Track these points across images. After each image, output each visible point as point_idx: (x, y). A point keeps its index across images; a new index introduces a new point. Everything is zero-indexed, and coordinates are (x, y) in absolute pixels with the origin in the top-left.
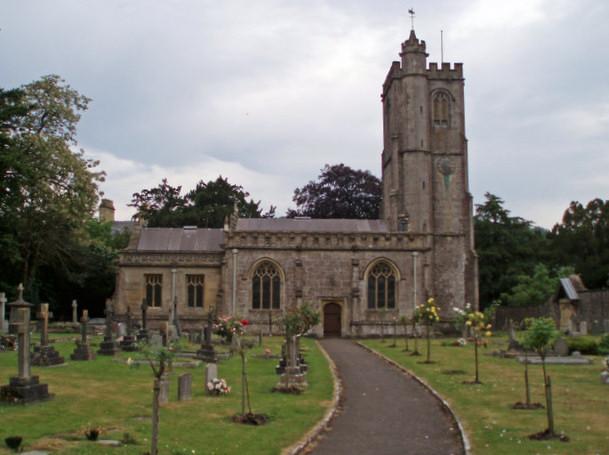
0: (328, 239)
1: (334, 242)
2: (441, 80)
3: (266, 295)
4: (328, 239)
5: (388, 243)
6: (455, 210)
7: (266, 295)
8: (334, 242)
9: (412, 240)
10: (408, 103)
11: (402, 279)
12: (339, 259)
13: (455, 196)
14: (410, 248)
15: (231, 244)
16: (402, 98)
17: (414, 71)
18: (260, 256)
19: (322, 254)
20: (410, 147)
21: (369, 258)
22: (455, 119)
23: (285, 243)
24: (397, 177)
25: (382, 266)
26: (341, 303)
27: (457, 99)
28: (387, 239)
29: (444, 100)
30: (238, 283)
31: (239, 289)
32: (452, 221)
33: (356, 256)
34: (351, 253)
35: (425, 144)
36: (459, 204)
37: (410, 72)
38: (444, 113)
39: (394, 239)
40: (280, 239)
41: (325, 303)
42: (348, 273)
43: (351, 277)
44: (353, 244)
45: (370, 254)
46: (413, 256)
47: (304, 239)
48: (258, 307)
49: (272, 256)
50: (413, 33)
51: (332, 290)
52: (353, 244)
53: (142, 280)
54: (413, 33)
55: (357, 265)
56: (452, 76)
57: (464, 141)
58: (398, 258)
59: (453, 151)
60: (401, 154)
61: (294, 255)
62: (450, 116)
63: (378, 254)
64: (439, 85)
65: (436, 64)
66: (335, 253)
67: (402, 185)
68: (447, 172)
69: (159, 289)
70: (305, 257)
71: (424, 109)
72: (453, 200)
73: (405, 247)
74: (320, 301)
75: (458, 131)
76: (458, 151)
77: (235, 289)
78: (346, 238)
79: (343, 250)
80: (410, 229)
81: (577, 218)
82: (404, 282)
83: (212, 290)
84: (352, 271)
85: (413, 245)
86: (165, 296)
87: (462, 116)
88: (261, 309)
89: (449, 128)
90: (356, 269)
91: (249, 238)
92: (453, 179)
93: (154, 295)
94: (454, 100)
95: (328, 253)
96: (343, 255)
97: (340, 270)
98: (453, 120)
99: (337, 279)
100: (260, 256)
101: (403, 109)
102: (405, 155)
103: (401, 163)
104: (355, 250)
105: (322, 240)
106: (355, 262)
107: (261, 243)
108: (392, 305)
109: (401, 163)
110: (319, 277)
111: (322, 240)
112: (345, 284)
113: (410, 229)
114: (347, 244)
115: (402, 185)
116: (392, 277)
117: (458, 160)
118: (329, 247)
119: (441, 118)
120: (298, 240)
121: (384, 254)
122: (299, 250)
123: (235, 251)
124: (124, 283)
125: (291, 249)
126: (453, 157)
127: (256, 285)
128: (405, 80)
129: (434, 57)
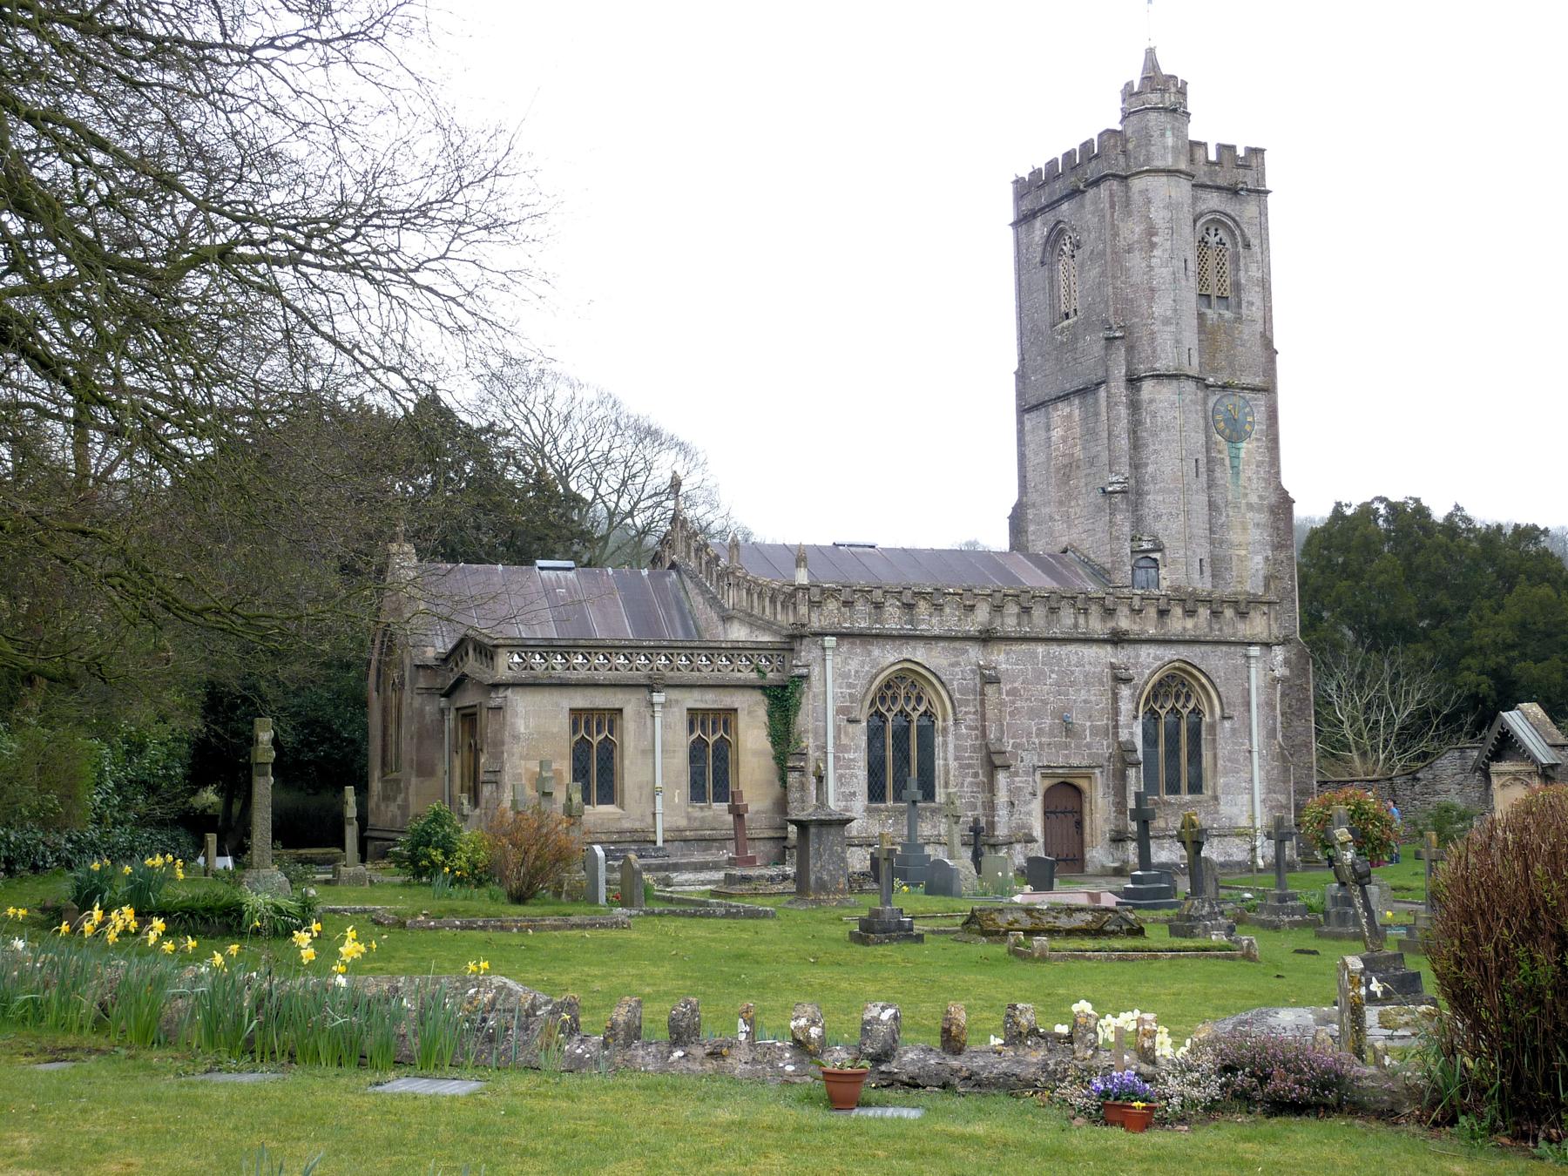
0: (1053, 610)
1: (1067, 618)
2: (1218, 188)
3: (1173, 752)
4: (1053, 610)
5: (1189, 623)
6: (1255, 535)
7: (1173, 752)
8: (1067, 618)
9: (1243, 615)
10: (1153, 246)
11: (1224, 718)
12: (1080, 664)
13: (1254, 499)
14: (1239, 637)
15: (816, 622)
16: (1132, 230)
17: (1169, 162)
18: (888, 657)
19: (1040, 649)
20: (1161, 366)
21: (1149, 662)
22: (1252, 295)
23: (951, 620)
24: (1124, 443)
25: (1174, 684)
26: (1083, 783)
27: (1254, 242)
28: (1190, 613)
29: (1220, 242)
30: (838, 729)
31: (839, 747)
32: (1252, 563)
33: (1120, 656)
34: (1109, 648)
35: (1195, 361)
36: (1263, 517)
37: (1159, 164)
38: (1220, 273)
39: (1204, 612)
40: (939, 608)
41: (1048, 783)
42: (1105, 702)
43: (1116, 712)
44: (1111, 624)
45: (1153, 650)
46: (1248, 657)
47: (998, 609)
48: (883, 799)
49: (920, 654)
50: (1150, 54)
51: (1067, 746)
52: (1111, 624)
53: (561, 724)
54: (1150, 54)
55: (1127, 681)
56: (1236, 179)
57: (1270, 352)
58: (1214, 661)
59: (1246, 380)
60: (1133, 381)
61: (975, 654)
62: (1237, 286)
63: (1169, 653)
64: (1213, 201)
65: (1232, 148)
66: (1072, 648)
67: (1136, 466)
68: (1235, 435)
69: (608, 753)
70: (1001, 658)
71: (1192, 266)
72: (1250, 507)
73: (1227, 633)
74: (1038, 777)
75: (1259, 327)
76: (1257, 381)
77: (830, 748)
78: (1094, 609)
79: (1088, 641)
80: (1168, 578)
81: (1345, 549)
82: (1227, 724)
83: (756, 753)
84: (1115, 698)
85: (1245, 630)
86: (632, 772)
87: (1265, 285)
88: (890, 803)
89: (1239, 319)
90: (1125, 692)
91: (832, 605)
92: (1248, 451)
93: (597, 767)
94: (1247, 246)
95: (1055, 649)
96: (1090, 652)
97: (1083, 695)
98: (1245, 297)
99: (1077, 719)
100: (888, 657)
101: (1136, 261)
102: (1147, 387)
103: (1135, 406)
104: (1118, 639)
105: (1039, 612)
106: (1124, 674)
107: (893, 619)
108: (1196, 787)
109: (1135, 406)
110: (1034, 713)
111: (1039, 612)
112: (1095, 731)
113: (1168, 578)
114: (1096, 625)
115: (1136, 466)
116: (1196, 712)
117: (1261, 400)
118: (1056, 631)
119: (1215, 293)
120: (982, 614)
121: (1183, 652)
122: (986, 638)
123: (830, 641)
124: (516, 737)
125: (968, 638)
126: (1248, 395)
127: (875, 735)
128: (1137, 184)
129: (1210, 125)
